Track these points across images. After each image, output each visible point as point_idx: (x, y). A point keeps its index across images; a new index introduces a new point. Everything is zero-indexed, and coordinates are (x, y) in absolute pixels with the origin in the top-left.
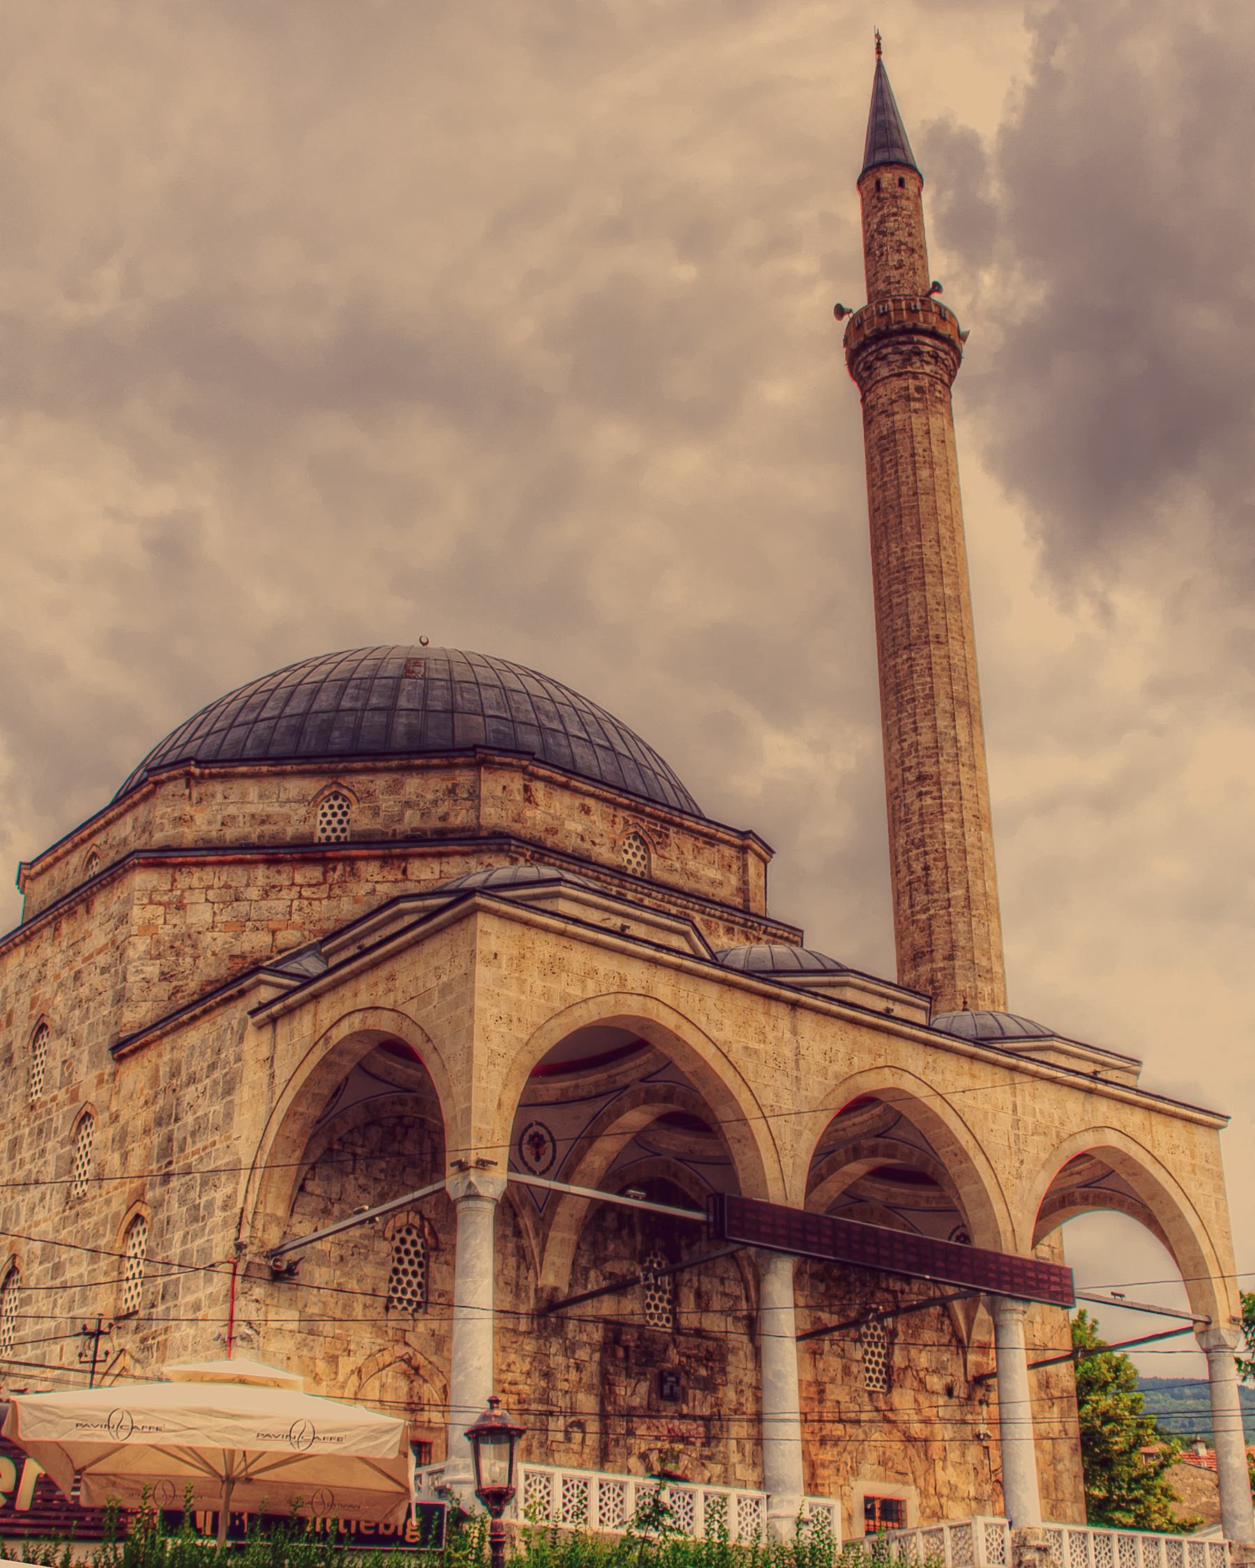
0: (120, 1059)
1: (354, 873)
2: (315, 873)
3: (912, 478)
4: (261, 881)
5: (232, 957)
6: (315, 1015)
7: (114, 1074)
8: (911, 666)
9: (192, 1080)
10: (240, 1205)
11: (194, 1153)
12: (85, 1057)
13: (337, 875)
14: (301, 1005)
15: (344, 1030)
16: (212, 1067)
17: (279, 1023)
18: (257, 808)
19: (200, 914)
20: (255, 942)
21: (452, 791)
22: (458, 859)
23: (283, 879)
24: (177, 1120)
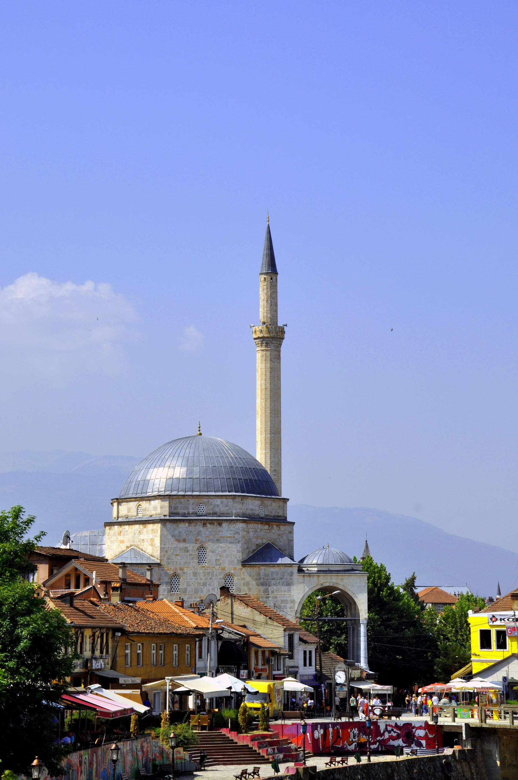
0: (243, 567)
1: (273, 527)
2: (266, 527)
3: (277, 384)
4: (260, 528)
5: (257, 545)
6: (318, 579)
7: (241, 569)
8: (274, 439)
9: (273, 579)
10: (296, 609)
11: (277, 595)
12: (227, 562)
13: (270, 528)
14: (313, 576)
15: (327, 584)
16: (281, 579)
17: (305, 577)
18: (251, 507)
19: (251, 534)
20: (259, 541)
21: (279, 507)
22: (287, 526)
23: (262, 528)
24: (269, 586)
